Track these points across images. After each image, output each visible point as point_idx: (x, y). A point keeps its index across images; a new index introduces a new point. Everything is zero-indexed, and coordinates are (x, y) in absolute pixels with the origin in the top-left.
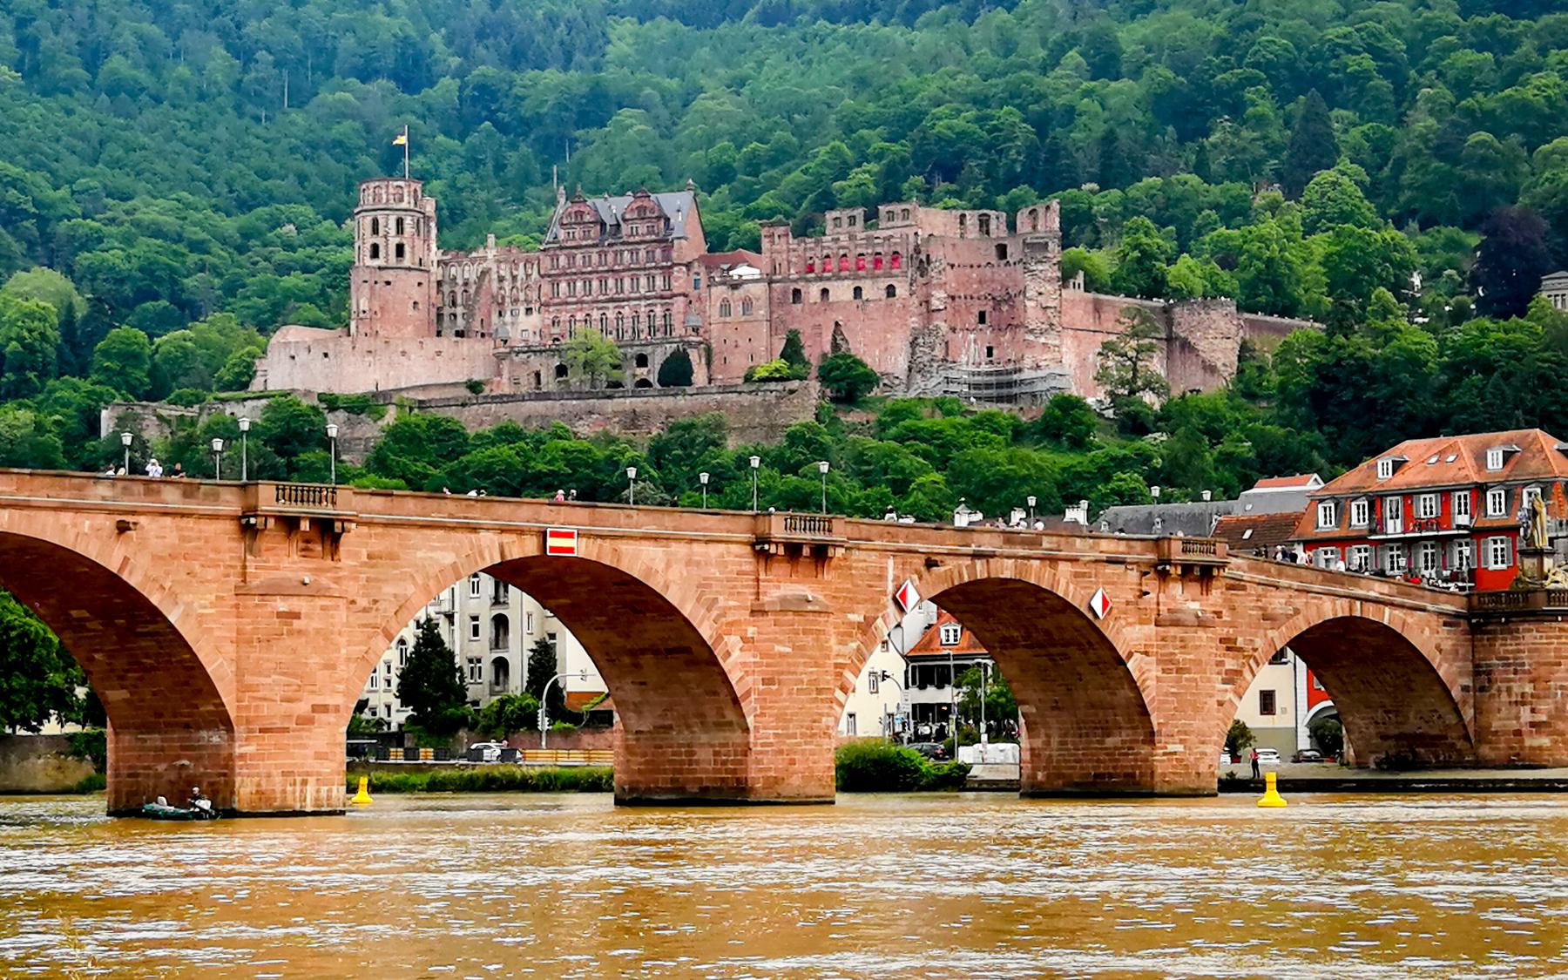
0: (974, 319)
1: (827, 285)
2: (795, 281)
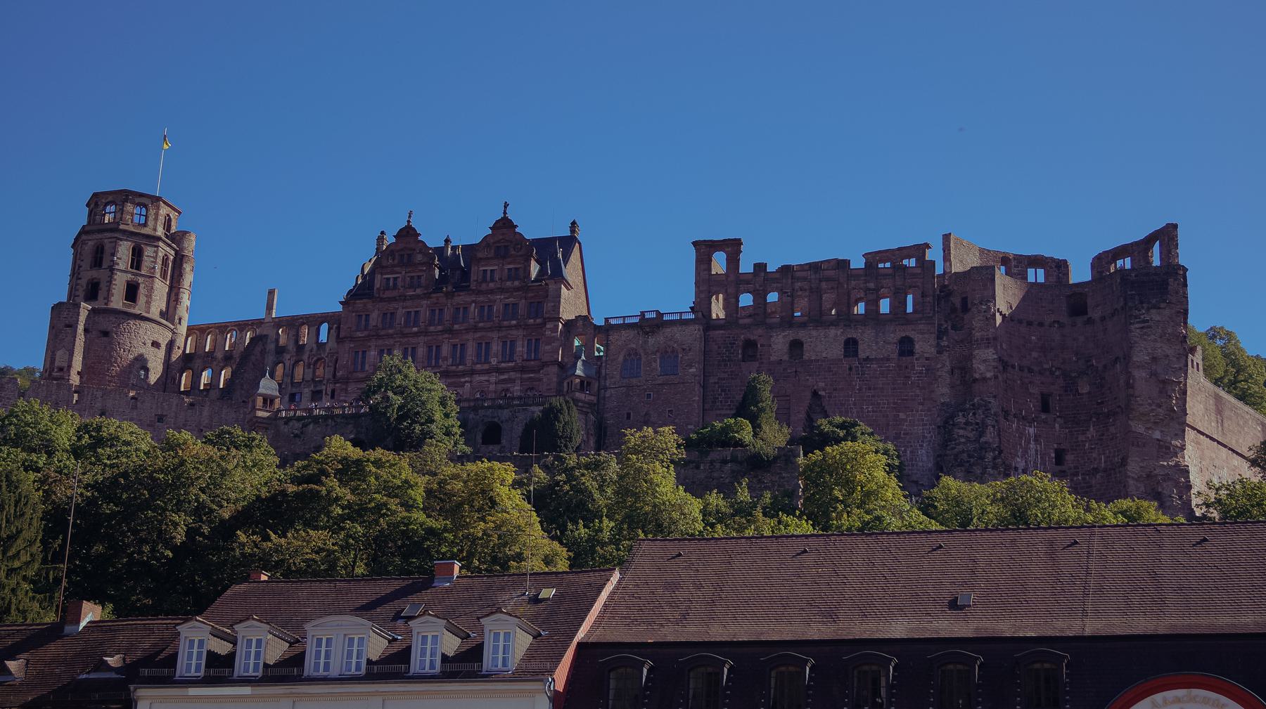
0: (1033, 405)
1: (802, 335)
2: (745, 327)
